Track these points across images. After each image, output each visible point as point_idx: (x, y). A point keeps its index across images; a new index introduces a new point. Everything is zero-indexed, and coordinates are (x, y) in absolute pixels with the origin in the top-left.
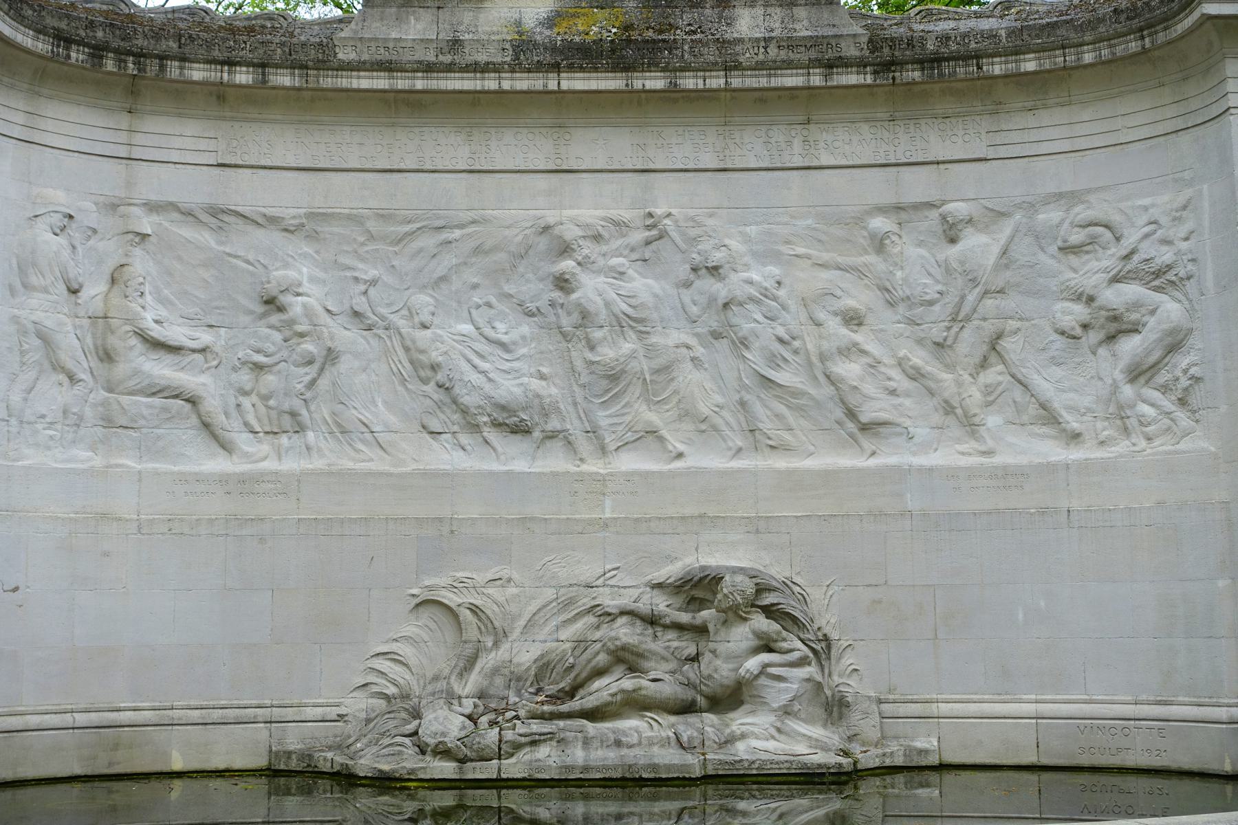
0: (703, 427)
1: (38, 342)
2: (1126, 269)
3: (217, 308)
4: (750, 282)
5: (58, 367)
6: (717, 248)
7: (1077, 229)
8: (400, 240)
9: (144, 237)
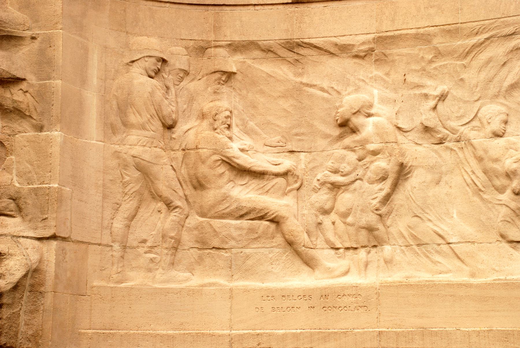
1: (137, 174)
3: (297, 135)
5: (156, 196)
8: (468, 53)
9: (230, 75)
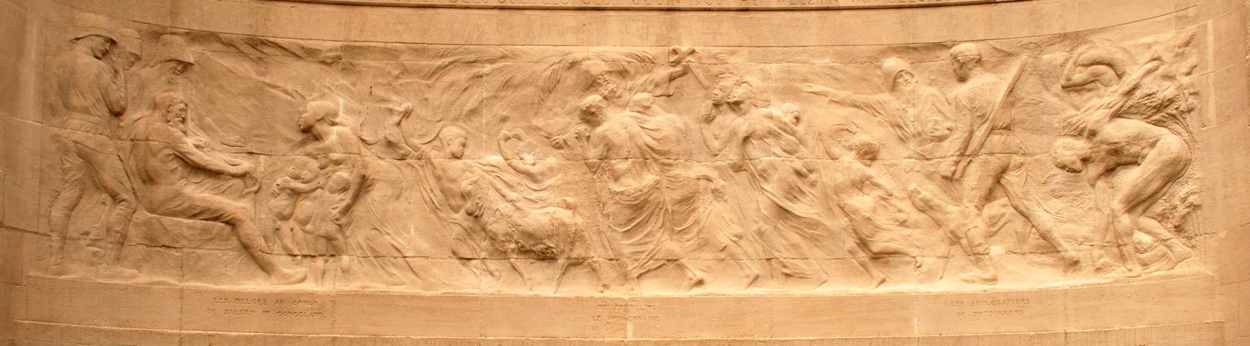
0: (722, 256)
2: (1127, 105)
3: (257, 136)
4: (771, 117)
6: (739, 84)
7: (1080, 68)
8: (433, 74)
9: (186, 66)
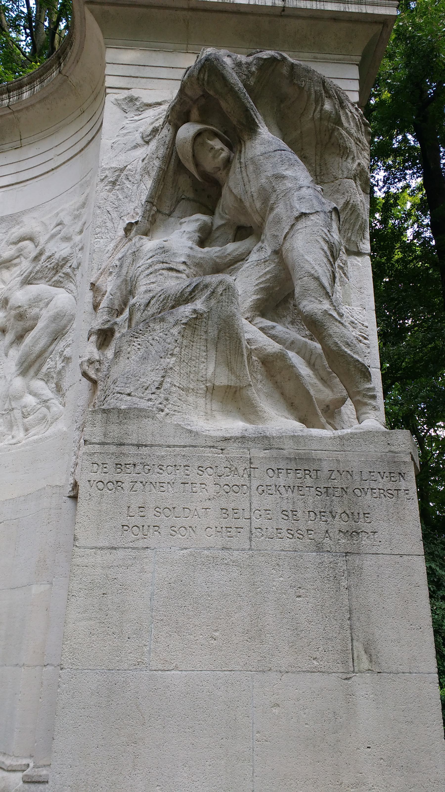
7: (11, 246)
